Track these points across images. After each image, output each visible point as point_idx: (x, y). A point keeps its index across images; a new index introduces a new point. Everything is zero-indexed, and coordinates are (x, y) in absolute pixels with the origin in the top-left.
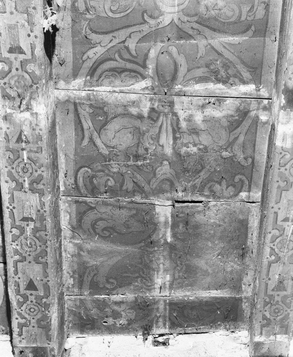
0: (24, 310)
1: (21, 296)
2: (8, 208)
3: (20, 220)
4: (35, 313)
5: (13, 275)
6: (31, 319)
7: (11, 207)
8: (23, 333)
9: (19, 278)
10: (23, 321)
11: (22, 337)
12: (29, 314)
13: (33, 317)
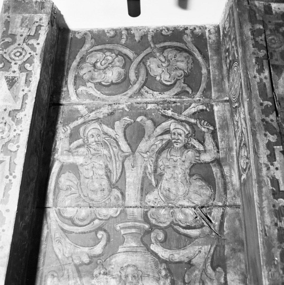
0: (28, 53)
1: (27, 70)
2: (15, 177)
3: (4, 161)
4: (16, 51)
5: (29, 94)
6: (21, 44)
7: (11, 177)
8: (35, 28)
9: (23, 90)
10: (32, 41)
11: (37, 24)
12: (23, 50)
13: (19, 46)
